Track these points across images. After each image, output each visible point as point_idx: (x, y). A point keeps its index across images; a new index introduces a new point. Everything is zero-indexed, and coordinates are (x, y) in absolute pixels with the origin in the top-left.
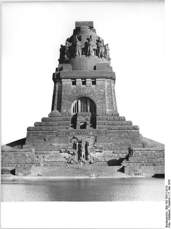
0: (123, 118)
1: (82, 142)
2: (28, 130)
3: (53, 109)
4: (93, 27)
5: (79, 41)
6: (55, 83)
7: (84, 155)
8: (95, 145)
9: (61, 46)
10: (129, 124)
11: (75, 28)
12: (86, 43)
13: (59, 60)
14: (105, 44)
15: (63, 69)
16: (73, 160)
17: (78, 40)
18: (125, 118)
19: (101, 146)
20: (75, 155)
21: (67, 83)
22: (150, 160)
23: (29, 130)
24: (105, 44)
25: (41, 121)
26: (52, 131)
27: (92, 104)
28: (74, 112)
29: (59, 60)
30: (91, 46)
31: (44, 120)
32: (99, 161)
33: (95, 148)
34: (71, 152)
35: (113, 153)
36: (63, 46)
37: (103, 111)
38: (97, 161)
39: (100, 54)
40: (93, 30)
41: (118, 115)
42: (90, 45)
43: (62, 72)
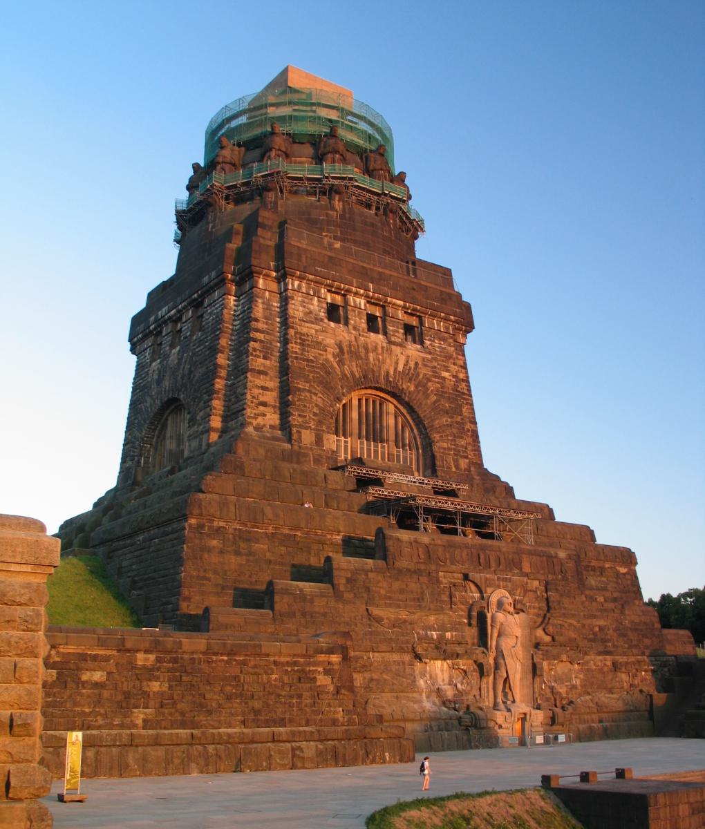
37: (457, 467)
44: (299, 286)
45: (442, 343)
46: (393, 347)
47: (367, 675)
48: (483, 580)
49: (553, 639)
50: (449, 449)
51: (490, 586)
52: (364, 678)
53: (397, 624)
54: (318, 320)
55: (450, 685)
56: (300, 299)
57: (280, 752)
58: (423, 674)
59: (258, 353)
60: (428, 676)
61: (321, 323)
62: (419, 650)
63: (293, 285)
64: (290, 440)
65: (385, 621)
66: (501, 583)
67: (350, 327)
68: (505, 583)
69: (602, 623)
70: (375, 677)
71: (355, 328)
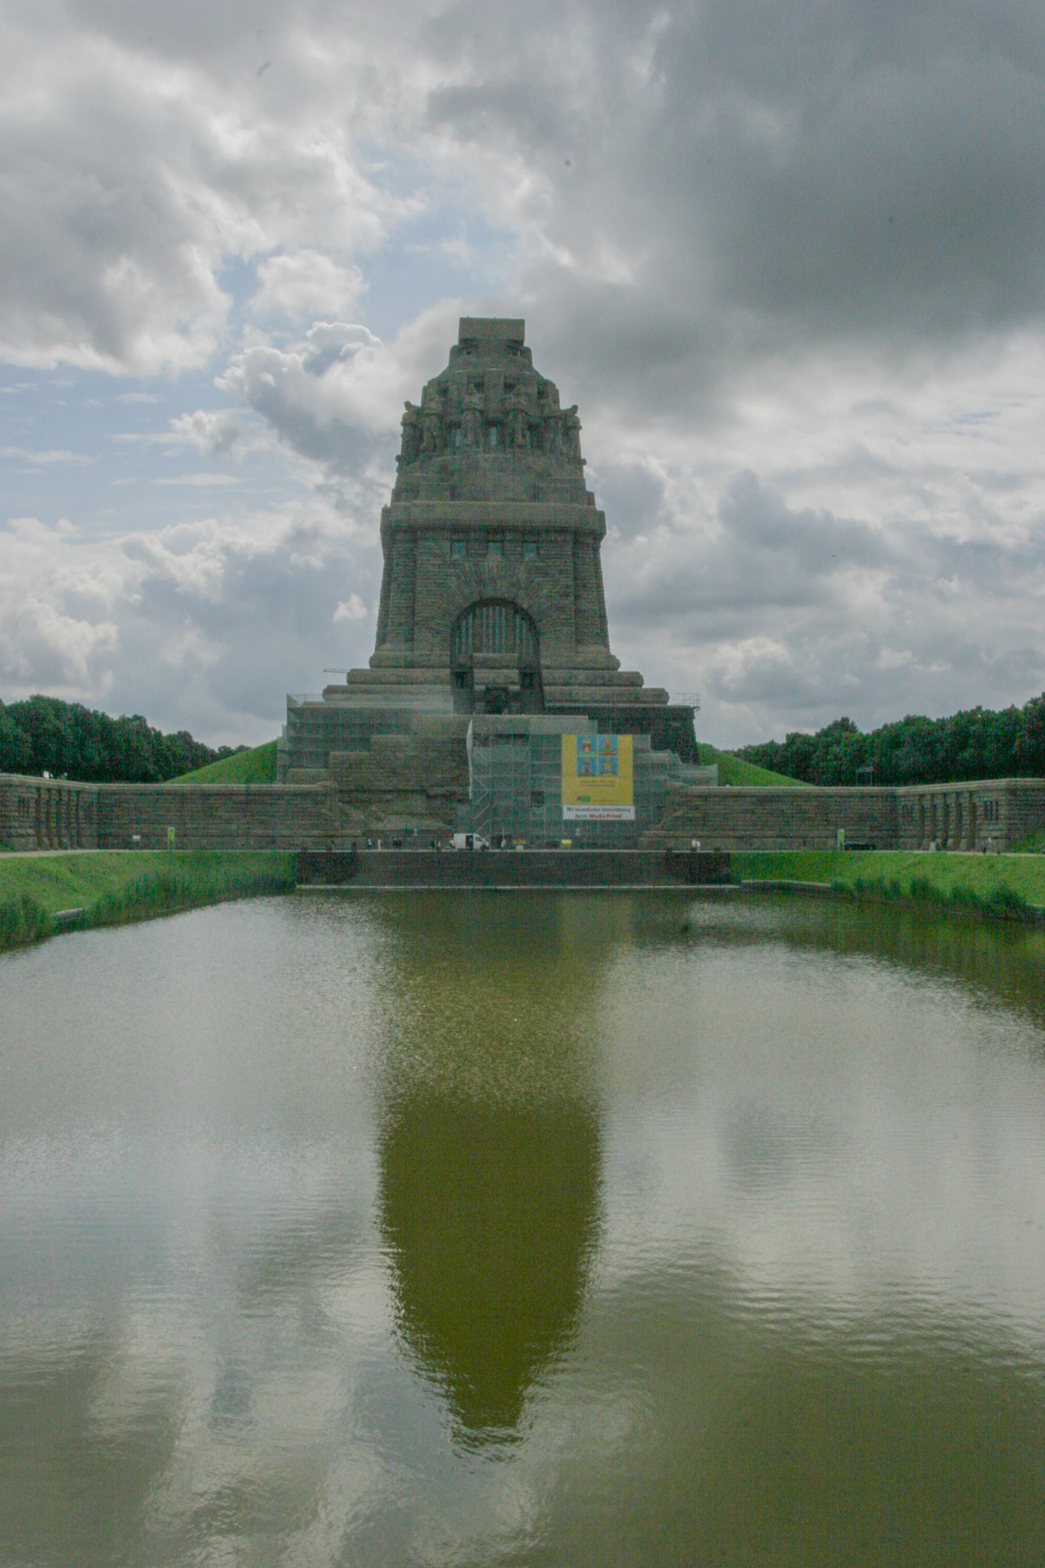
3: (382, 639)
4: (522, 342)
9: (408, 405)
11: (456, 342)
12: (503, 401)
13: (398, 458)
14: (564, 405)
15: (422, 494)
17: (472, 386)
18: (640, 678)
24: (564, 405)
29: (398, 458)
31: (354, 677)
36: (414, 407)
39: (547, 445)
41: (613, 664)
43: (415, 505)
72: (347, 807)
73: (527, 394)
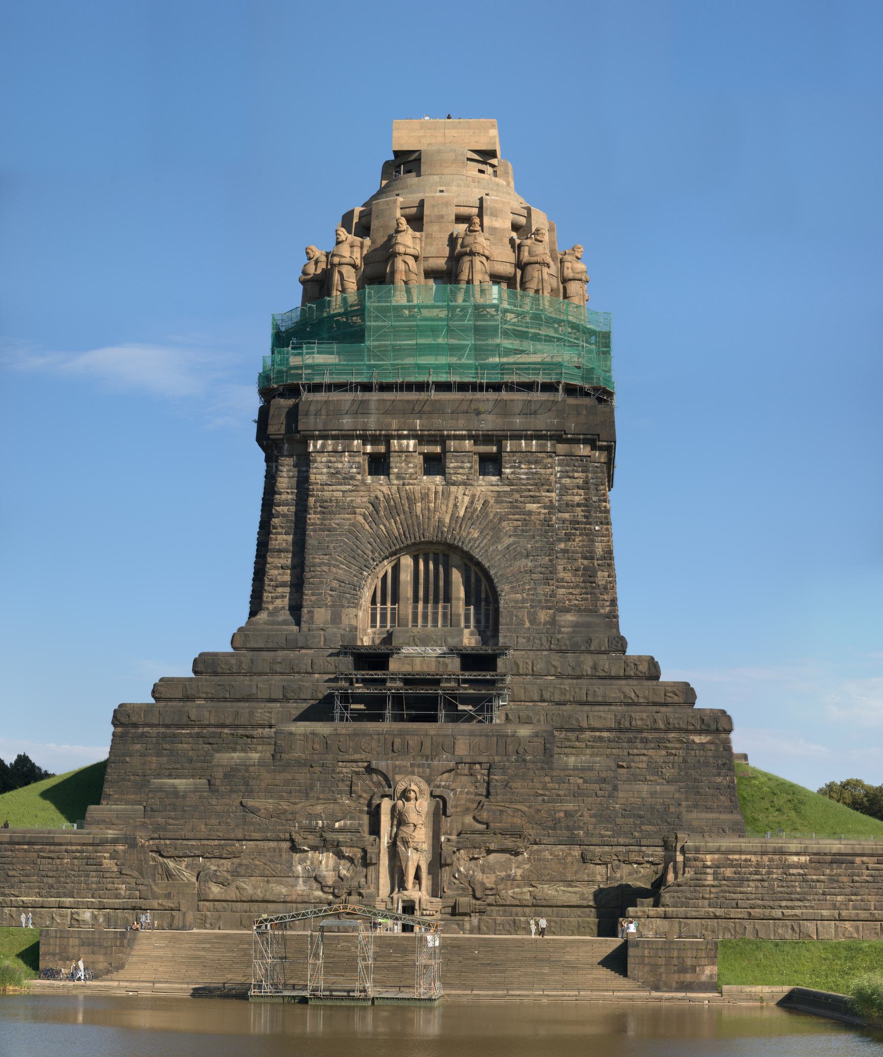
0: (646, 665)
1: (412, 795)
2: (116, 722)
5: (410, 231)
6: (271, 460)
7: (418, 869)
8: (485, 816)
10: (676, 699)
16: (360, 894)
19: (518, 821)
20: (371, 864)
21: (334, 466)
22: (777, 903)
23: (123, 720)
25: (192, 675)
26: (250, 732)
27: (478, 581)
28: (373, 626)
30: (477, 260)
31: (205, 664)
32: (501, 902)
33: (481, 833)
34: (347, 852)
35: (584, 859)
37: (533, 621)
38: (491, 899)
40: (493, 166)
42: (472, 254)
44: (323, 446)
45: (533, 466)
46: (453, 489)
47: (236, 861)
48: (391, 768)
49: (487, 825)
50: (524, 601)
51: (400, 773)
52: (233, 864)
53: (278, 814)
54: (348, 478)
55: (334, 870)
56: (324, 459)
57: (61, 915)
58: (302, 861)
59: (280, 530)
60: (308, 862)
61: (351, 482)
62: (297, 838)
63: (315, 446)
64: (298, 623)
65: (263, 811)
66: (416, 770)
67: (392, 476)
68: (421, 770)
69: (570, 807)
70: (245, 862)
71: (399, 477)
72: (171, 864)
73: (493, 230)
